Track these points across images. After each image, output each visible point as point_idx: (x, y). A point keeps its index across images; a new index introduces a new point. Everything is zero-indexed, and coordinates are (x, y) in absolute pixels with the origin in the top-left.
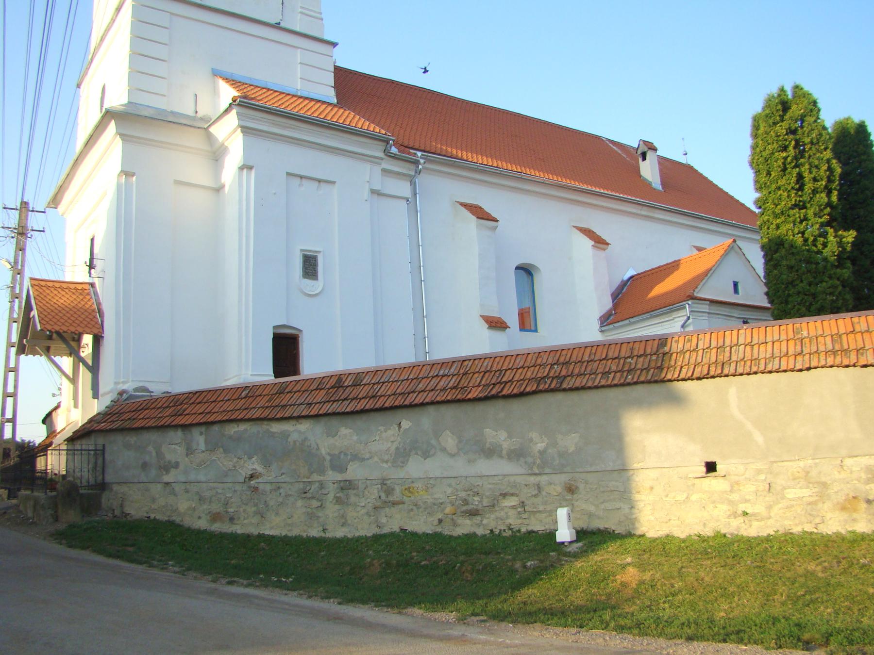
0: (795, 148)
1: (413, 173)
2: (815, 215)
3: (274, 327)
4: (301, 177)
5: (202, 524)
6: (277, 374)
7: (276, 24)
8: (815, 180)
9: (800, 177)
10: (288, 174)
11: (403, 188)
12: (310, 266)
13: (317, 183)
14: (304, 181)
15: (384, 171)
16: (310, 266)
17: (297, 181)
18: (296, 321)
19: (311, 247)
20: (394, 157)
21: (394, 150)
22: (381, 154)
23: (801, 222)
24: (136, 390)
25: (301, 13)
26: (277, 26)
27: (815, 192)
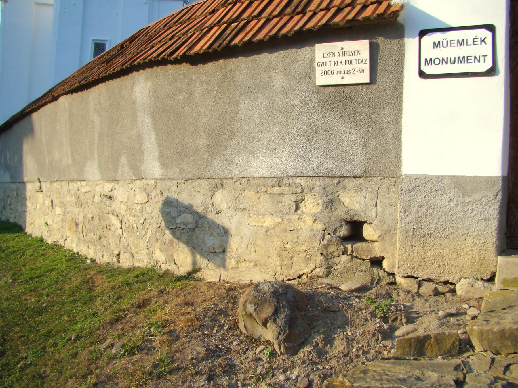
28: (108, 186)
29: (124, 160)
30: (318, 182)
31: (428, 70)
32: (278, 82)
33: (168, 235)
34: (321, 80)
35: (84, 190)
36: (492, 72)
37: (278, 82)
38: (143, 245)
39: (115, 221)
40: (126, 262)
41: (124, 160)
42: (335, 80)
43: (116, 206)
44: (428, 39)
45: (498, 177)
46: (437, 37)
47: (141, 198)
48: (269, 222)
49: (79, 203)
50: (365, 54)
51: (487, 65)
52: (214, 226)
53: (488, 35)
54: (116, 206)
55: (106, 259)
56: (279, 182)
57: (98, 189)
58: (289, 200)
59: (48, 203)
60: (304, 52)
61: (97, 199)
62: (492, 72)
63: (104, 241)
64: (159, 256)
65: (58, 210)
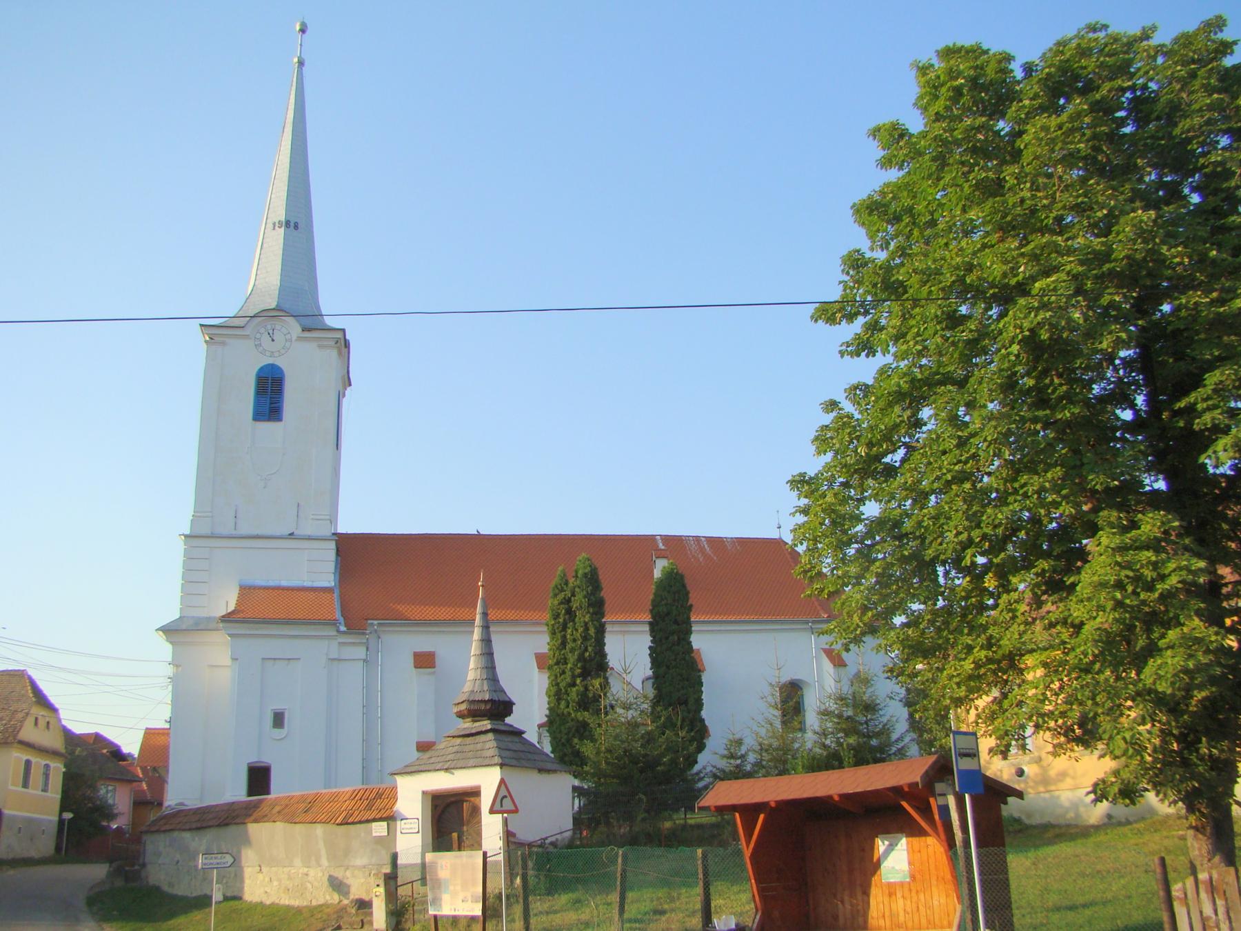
0: (565, 615)
1: (365, 641)
2: (571, 668)
3: (248, 764)
4: (275, 659)
5: (166, 888)
6: (250, 793)
7: (290, 534)
8: (574, 640)
9: (564, 637)
10: (263, 659)
11: (360, 652)
12: (279, 719)
13: (286, 662)
14: (277, 661)
15: (339, 643)
16: (279, 719)
17: (272, 661)
18: (266, 759)
19: (278, 706)
20: (344, 633)
21: (343, 628)
22: (335, 633)
23: (561, 675)
24: (176, 805)
25: (313, 519)
26: (291, 535)
27: (572, 650)
28: (306, 870)
29: (313, 858)
30: (376, 867)
31: (403, 831)
32: (363, 834)
33: (331, 890)
34: (374, 834)
35: (293, 871)
36: (418, 832)
37: (363, 834)
38: (322, 894)
39: (309, 886)
40: (314, 903)
41: (313, 858)
42: (378, 834)
43: (310, 878)
44: (403, 822)
45: (411, 865)
46: (405, 821)
47: (320, 874)
48: (363, 880)
49: (290, 878)
50: (386, 827)
51: (417, 830)
52: (345, 884)
53: (416, 821)
54: (310, 878)
55: (305, 904)
56: (364, 867)
57: (301, 871)
58: (367, 873)
59: (267, 879)
60: (369, 825)
61: (300, 875)
62: (418, 832)
63: (304, 896)
64: (328, 897)
65: (275, 883)
